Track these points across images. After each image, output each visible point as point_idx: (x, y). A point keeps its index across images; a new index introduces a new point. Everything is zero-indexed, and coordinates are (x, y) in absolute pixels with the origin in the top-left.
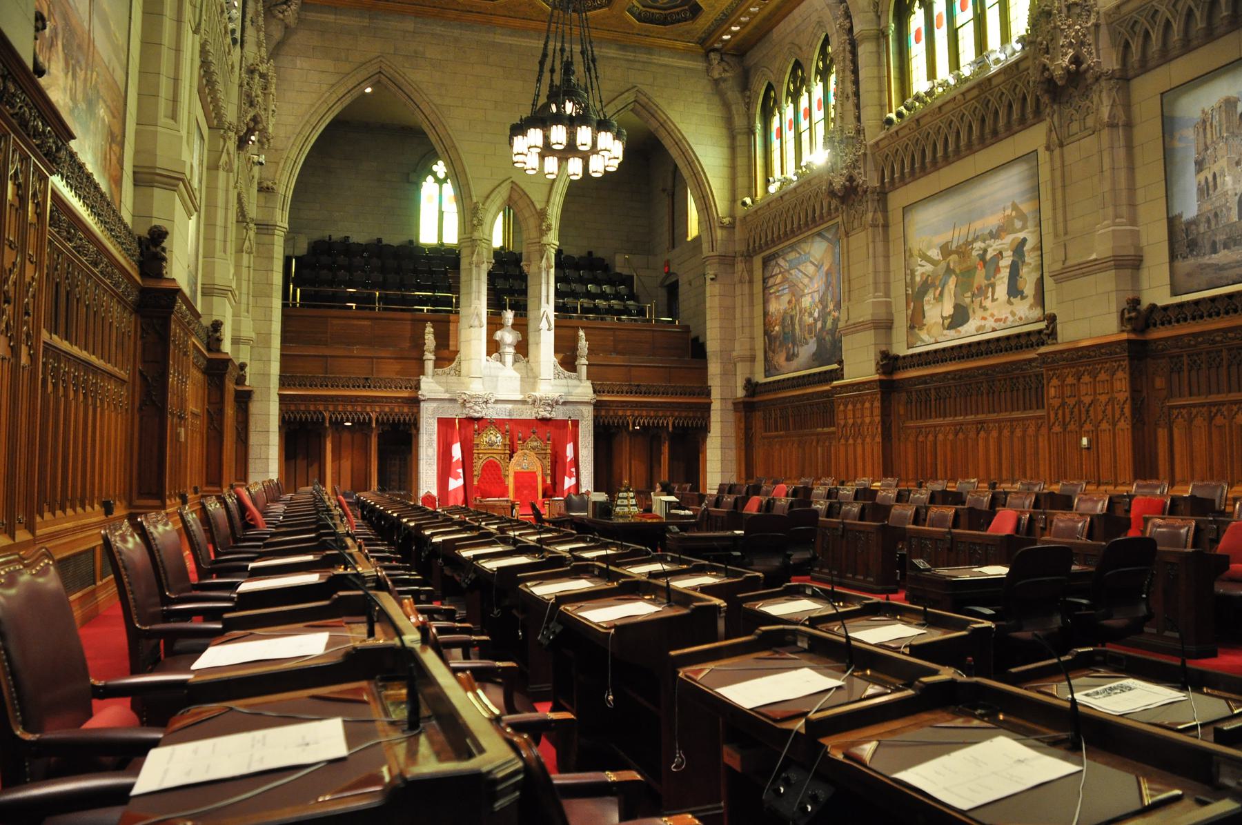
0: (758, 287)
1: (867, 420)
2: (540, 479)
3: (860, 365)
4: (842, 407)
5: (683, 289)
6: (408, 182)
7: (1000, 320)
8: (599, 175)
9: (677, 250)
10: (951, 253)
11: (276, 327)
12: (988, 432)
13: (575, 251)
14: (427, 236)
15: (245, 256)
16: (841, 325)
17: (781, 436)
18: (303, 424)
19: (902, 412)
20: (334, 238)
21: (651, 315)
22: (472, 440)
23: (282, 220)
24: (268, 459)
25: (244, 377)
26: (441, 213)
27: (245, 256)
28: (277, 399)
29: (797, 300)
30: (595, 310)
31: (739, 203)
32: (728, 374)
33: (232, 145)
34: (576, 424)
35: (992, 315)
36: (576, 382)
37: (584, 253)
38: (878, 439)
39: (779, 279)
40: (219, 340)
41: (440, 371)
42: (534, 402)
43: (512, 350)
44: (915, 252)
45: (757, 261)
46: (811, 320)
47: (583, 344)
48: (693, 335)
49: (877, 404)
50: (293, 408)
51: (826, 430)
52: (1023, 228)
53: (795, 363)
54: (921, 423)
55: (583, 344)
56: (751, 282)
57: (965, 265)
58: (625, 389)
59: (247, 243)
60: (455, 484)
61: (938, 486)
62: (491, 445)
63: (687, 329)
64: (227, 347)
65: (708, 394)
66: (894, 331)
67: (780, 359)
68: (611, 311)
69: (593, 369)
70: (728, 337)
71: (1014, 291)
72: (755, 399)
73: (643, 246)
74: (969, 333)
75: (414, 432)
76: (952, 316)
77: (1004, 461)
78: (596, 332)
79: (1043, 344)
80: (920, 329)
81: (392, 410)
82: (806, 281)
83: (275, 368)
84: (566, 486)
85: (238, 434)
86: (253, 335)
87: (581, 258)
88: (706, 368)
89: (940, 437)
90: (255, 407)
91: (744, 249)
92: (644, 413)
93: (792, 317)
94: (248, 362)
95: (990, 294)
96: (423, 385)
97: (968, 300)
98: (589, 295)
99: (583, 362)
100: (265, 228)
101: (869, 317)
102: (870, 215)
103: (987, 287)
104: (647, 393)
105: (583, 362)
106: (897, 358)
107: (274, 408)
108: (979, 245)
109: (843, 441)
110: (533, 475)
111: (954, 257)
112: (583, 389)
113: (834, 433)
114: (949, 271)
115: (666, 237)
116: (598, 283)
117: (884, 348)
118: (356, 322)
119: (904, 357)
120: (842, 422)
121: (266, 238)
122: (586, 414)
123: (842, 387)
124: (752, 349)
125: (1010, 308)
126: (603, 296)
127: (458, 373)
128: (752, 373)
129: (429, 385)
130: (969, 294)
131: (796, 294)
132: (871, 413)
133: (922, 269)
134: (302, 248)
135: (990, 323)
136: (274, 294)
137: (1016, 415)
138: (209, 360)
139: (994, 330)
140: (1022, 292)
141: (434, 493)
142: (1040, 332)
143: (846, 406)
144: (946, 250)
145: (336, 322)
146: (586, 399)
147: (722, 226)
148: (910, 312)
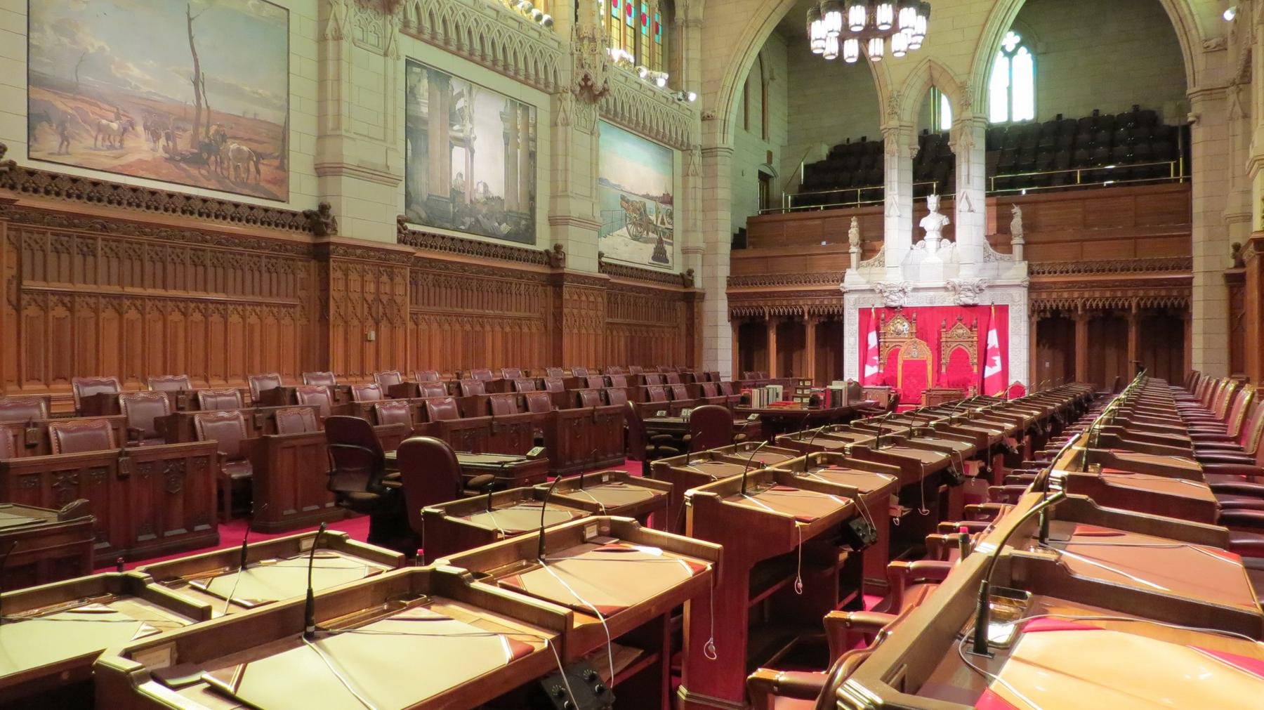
2: (929, 368)
8: (854, 60)
13: (1113, 106)
18: (752, 318)
20: (852, 141)
21: (1177, 173)
23: (728, 139)
25: (692, 283)
27: (691, 178)
33: (569, 103)
34: (1003, 310)
36: (1008, 264)
37: (1128, 109)
41: (864, 263)
47: (1017, 224)
55: (1017, 224)
58: (1070, 267)
59: (692, 167)
65: (1189, 267)
83: (724, 271)
85: (688, 329)
90: (707, 305)
92: (1097, 294)
96: (847, 278)
99: (1017, 241)
100: (708, 152)
110: (923, 364)
112: (1016, 270)
118: (809, 223)
121: (710, 160)
122: (1017, 299)
129: (855, 278)
138: (551, 275)
145: (792, 223)
146: (1018, 282)
147: (1208, 51)
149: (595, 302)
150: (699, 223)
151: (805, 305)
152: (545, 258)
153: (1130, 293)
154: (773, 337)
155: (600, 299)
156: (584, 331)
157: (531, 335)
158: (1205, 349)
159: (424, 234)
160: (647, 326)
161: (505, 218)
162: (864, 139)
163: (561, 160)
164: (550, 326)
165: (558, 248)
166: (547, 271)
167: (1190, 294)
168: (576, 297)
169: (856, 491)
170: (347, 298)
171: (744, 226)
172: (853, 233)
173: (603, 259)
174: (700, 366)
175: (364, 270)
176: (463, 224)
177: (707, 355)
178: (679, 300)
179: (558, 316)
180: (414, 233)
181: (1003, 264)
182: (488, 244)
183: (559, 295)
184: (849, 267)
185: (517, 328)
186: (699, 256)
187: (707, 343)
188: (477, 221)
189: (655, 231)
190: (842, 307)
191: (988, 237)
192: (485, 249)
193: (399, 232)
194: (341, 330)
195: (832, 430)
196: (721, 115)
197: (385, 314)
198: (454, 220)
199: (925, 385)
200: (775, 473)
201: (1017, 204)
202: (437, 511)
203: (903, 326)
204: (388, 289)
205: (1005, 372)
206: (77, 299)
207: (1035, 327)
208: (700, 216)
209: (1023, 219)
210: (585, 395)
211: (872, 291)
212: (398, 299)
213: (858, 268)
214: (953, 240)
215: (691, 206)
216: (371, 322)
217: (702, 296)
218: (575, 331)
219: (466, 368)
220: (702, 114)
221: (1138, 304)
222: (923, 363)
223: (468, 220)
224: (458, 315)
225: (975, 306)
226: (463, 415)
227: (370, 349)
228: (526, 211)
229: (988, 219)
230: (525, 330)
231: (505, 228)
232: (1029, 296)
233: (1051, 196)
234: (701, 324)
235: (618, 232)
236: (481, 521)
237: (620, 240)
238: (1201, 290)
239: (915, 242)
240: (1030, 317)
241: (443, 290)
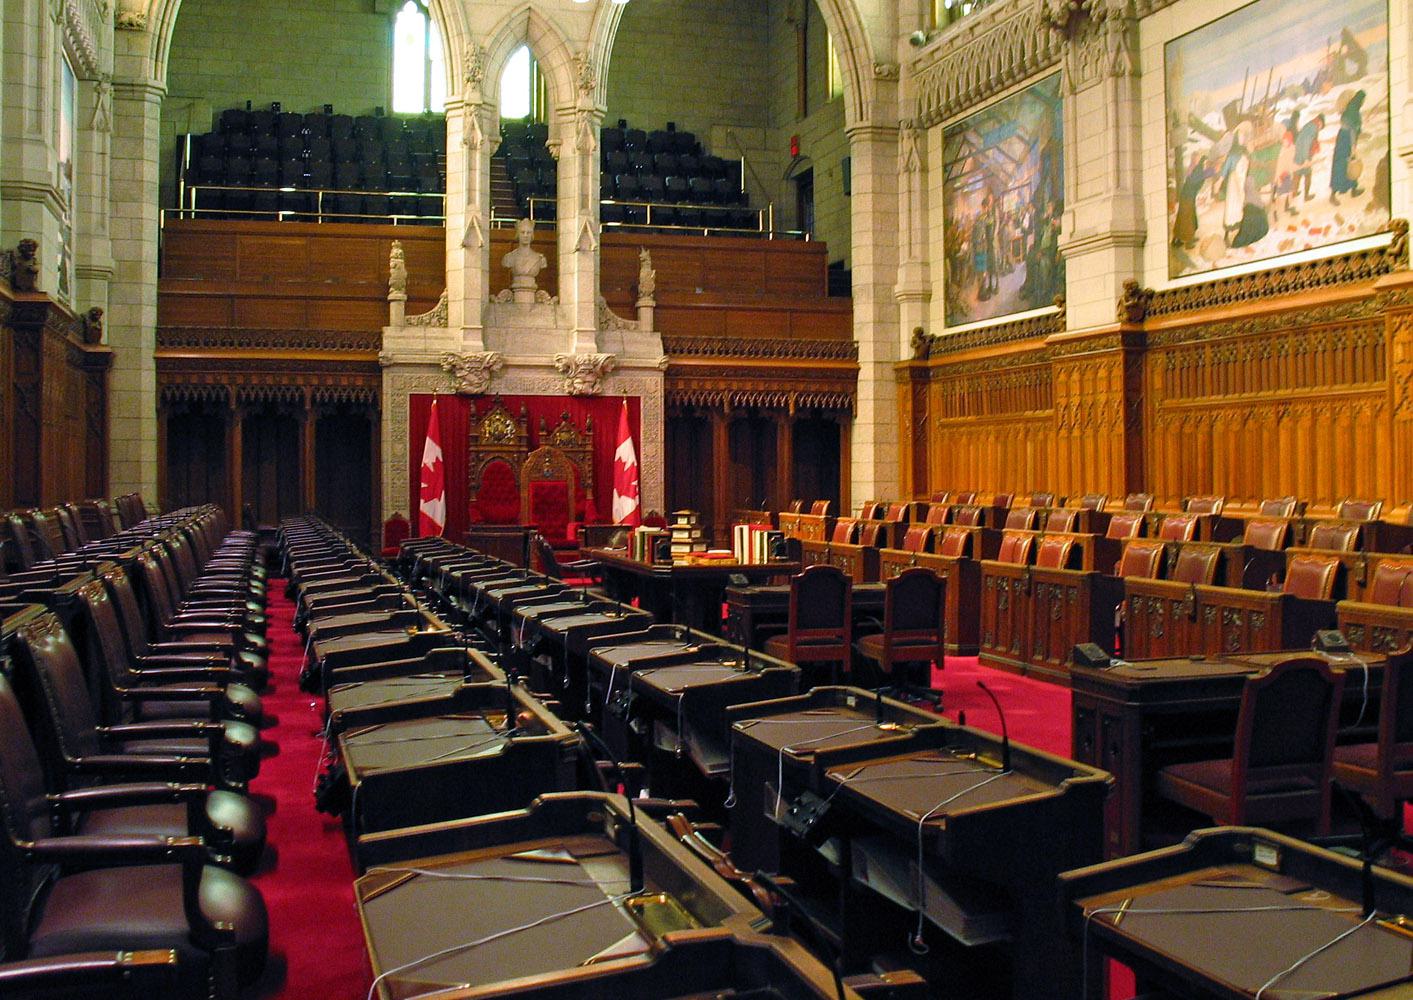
0: (936, 177)
1: (1102, 398)
2: (571, 493)
3: (1092, 305)
4: (1062, 377)
5: (820, 183)
6: (374, 12)
7: (1314, 232)
9: (811, 118)
10: (1241, 118)
11: (150, 250)
12: (1295, 420)
13: (645, 120)
14: (406, 101)
15: (96, 137)
16: (1062, 240)
17: (971, 424)
18: (196, 405)
19: (1158, 382)
20: (255, 106)
21: (766, 226)
22: (468, 430)
23: (156, 75)
25: (98, 333)
26: (428, 62)
27: (96, 137)
28: (152, 365)
29: (996, 200)
30: (676, 217)
31: (906, 40)
32: (885, 321)
34: (634, 402)
35: (1306, 223)
37: (663, 127)
38: (1120, 428)
39: (968, 164)
40: (33, 274)
41: (414, 319)
42: (567, 368)
43: (531, 282)
44: (1183, 118)
45: (935, 136)
46: (1018, 233)
47: (647, 275)
48: (832, 257)
49: (1118, 372)
50: (179, 380)
51: (1039, 413)
52: (1360, 74)
53: (991, 304)
54: (1187, 402)
56: (924, 170)
57: (1261, 140)
58: (717, 346)
59: (99, 113)
63: (821, 249)
64: (48, 283)
66: (1148, 250)
67: (970, 296)
68: (703, 219)
70: (886, 263)
71: (1343, 182)
72: (930, 363)
73: (756, 112)
74: (1266, 255)
75: (374, 418)
76: (1241, 225)
77: (1320, 468)
78: (673, 254)
79: (1387, 271)
80: (1190, 247)
82: (1010, 167)
83: (149, 316)
87: (656, 134)
88: (849, 312)
89: (1219, 427)
90: (118, 380)
91: (914, 116)
93: (988, 228)
94: (104, 307)
95: (1302, 187)
96: (386, 343)
97: (1266, 198)
98: (667, 194)
99: (646, 304)
100: (128, 89)
101: (1104, 228)
102: (1112, 56)
103: (1298, 176)
104: (754, 353)
105: (646, 304)
106: (1151, 295)
107: (148, 380)
108: (1285, 105)
109: (1063, 432)
111: (1245, 127)
112: (645, 347)
113: (1049, 418)
114: (1237, 149)
115: (793, 97)
116: (680, 172)
117: (1129, 277)
118: (282, 241)
119: (1163, 295)
120: (1063, 401)
121: (131, 106)
123: (1063, 342)
124: (926, 281)
125: (1333, 211)
126: (688, 195)
127: (444, 322)
128: (926, 319)
129: (402, 339)
130: (1268, 188)
131: (995, 191)
132: (1107, 388)
133: (1197, 147)
134: (204, 121)
135: (1302, 237)
136: (146, 197)
137: (1340, 389)
138: (15, 304)
139: (1308, 248)
140: (1354, 184)
141: (406, 515)
142: (1382, 251)
143: (1069, 375)
144: (1232, 115)
148: (1173, 218)
153: (788, 387)
158: (878, 463)
162: (328, 108)
163: (29, 65)
167: (856, 391)
181: (628, 335)
184: (388, 325)
196: (153, 27)
201: (647, 247)
203: (499, 425)
206: (236, 301)
211: (437, 366)
215: (96, 189)
220: (117, 17)
221: (796, 402)
225: (595, 398)
233: (724, 242)
238: (871, 385)
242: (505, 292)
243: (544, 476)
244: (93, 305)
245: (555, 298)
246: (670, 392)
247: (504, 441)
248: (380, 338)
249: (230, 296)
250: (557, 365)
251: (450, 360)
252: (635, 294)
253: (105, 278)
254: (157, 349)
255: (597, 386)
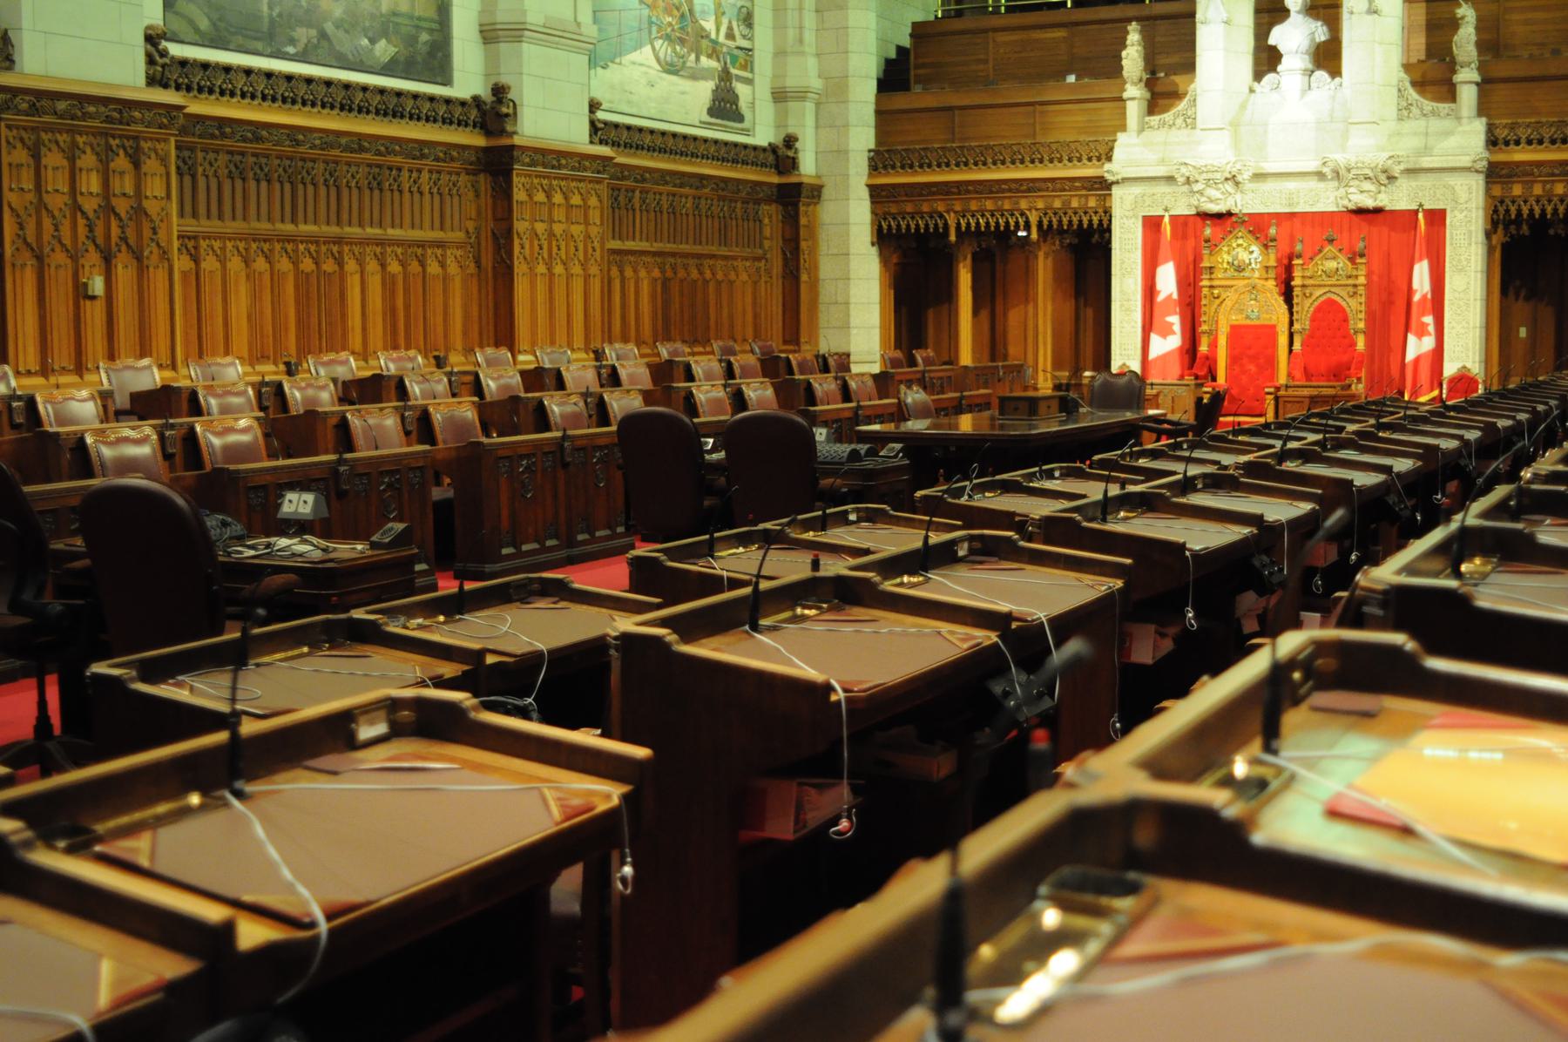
2: (1283, 340)
22: (1197, 259)
24: (847, 303)
28: (865, 194)
34: (1437, 218)
36: (1448, 124)
41: (1154, 120)
43: (1304, 62)
47: (1466, 40)
50: (894, 209)
55: (1466, 40)
60: (1166, 344)
61: (351, 367)
62: (1240, 269)
69: (1501, 92)
81: (1067, 203)
83: (862, 137)
84: (1410, 355)
86: (816, 83)
90: (827, 212)
96: (1117, 154)
99: (1467, 78)
105: (1467, 78)
110: (1271, 330)
112: (1462, 136)
122: (1463, 196)
127: (1190, 122)
138: (486, 150)
146: (1465, 161)
149: (586, 208)
150: (809, 37)
151: (1034, 209)
152: (474, 114)
154: (965, 278)
155: (593, 201)
156: (559, 269)
157: (446, 279)
159: (205, 66)
160: (699, 256)
161: (385, 27)
164: (487, 261)
165: (499, 91)
166: (478, 140)
168: (540, 197)
169: (1008, 617)
170: (41, 206)
171: (906, 42)
172: (1132, 57)
173: (600, 115)
174: (813, 337)
175: (74, 145)
176: (292, 42)
177: (827, 316)
178: (769, 201)
179: (503, 238)
180: (183, 63)
181: (1435, 124)
182: (347, 86)
183: (503, 192)
184: (1123, 128)
185: (415, 267)
186: (809, 107)
187: (827, 291)
188: (323, 35)
189: (714, 53)
190: (1108, 212)
191: (1407, 67)
192: (340, 96)
193: (150, 61)
194: (29, 276)
195: (1049, 475)
197: (124, 239)
198: (270, 36)
199: (1273, 375)
200: (839, 579)
202: (116, 672)
204: (130, 190)
205: (1438, 353)
207: (1498, 254)
208: (810, 20)
209: (1477, 29)
210: (556, 406)
211: (1170, 179)
212: (151, 207)
213: (1141, 130)
214: (1335, 72)
216: (93, 257)
217: (816, 192)
218: (541, 269)
219: (304, 350)
222: (1271, 330)
223: (303, 34)
224: (290, 239)
225: (1378, 211)
226: (272, 455)
227: (94, 314)
228: (431, 13)
229: (1408, 30)
230: (433, 268)
231: (384, 50)
232: (1488, 190)
234: (814, 249)
235: (635, 56)
236: (199, 691)
237: (636, 73)
239: (1258, 76)
240: (1488, 235)
241: (252, 185)
242: (1269, 78)
243: (1248, 317)
244: (791, 130)
245: (1337, 80)
246: (1502, 202)
247: (1247, 274)
248: (1112, 149)
249: (951, 109)
250: (1325, 170)
251: (1184, 170)
252: (1452, 66)
253: (803, 99)
254: (870, 175)
255: (1380, 196)
